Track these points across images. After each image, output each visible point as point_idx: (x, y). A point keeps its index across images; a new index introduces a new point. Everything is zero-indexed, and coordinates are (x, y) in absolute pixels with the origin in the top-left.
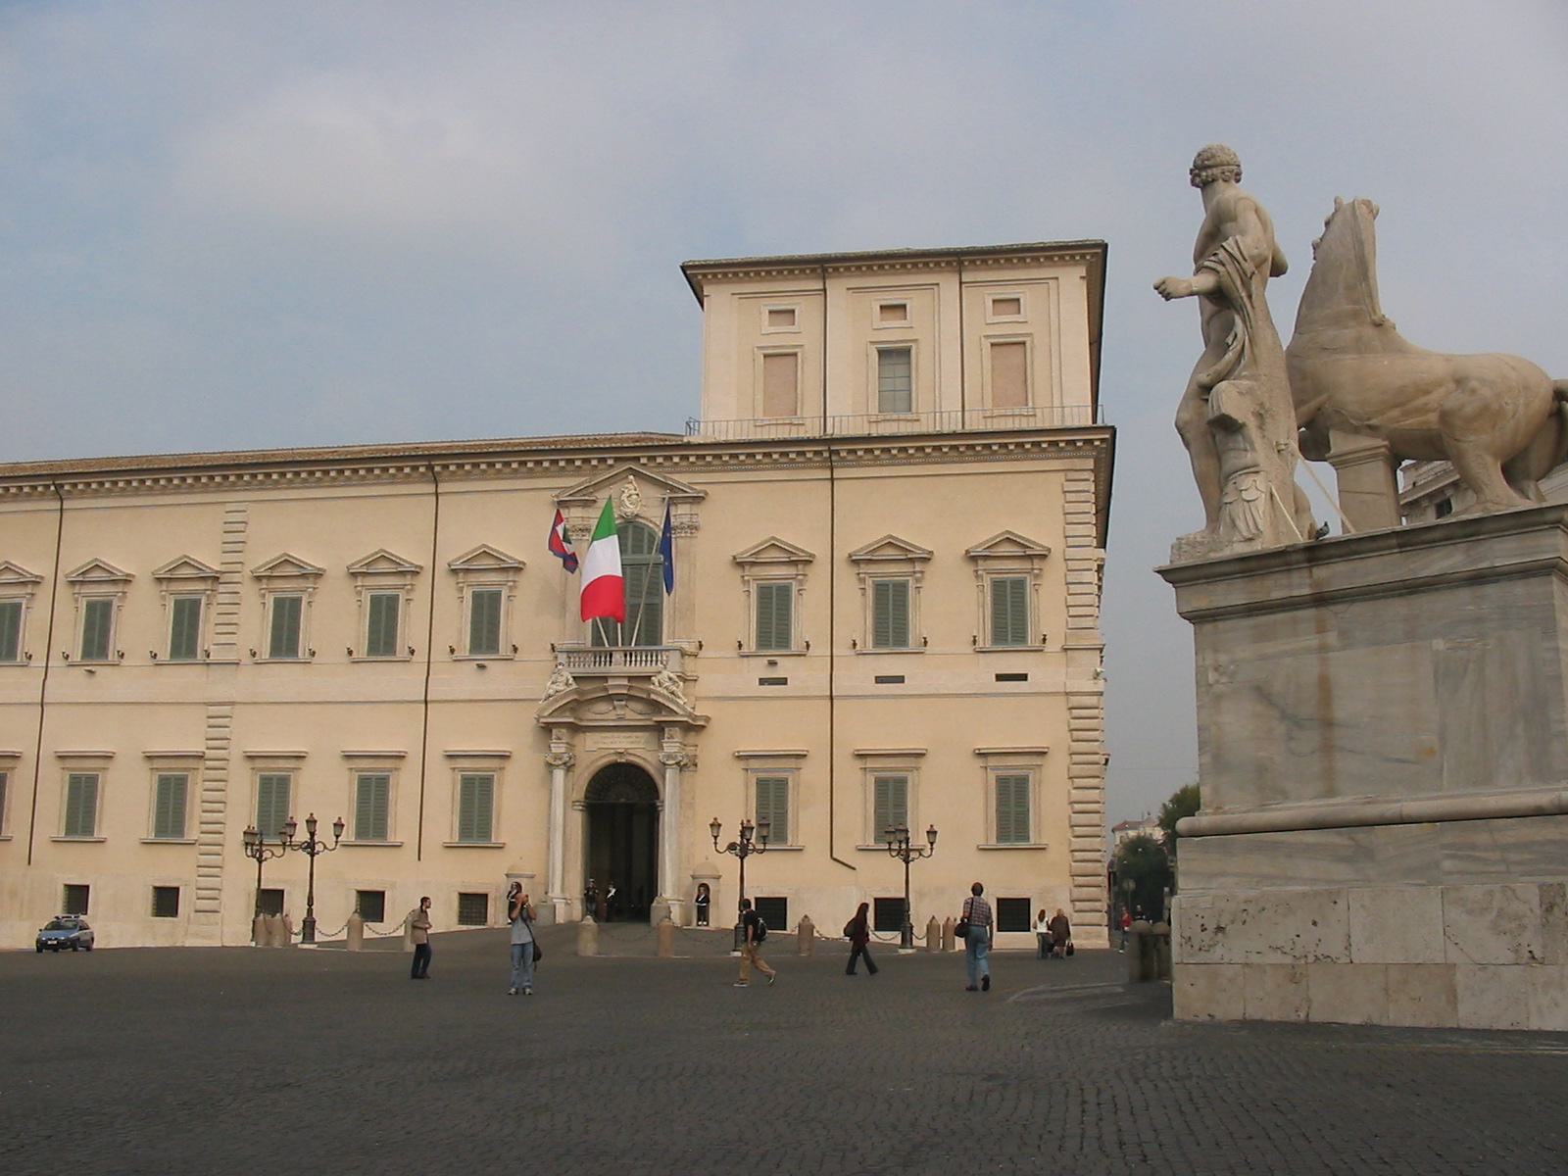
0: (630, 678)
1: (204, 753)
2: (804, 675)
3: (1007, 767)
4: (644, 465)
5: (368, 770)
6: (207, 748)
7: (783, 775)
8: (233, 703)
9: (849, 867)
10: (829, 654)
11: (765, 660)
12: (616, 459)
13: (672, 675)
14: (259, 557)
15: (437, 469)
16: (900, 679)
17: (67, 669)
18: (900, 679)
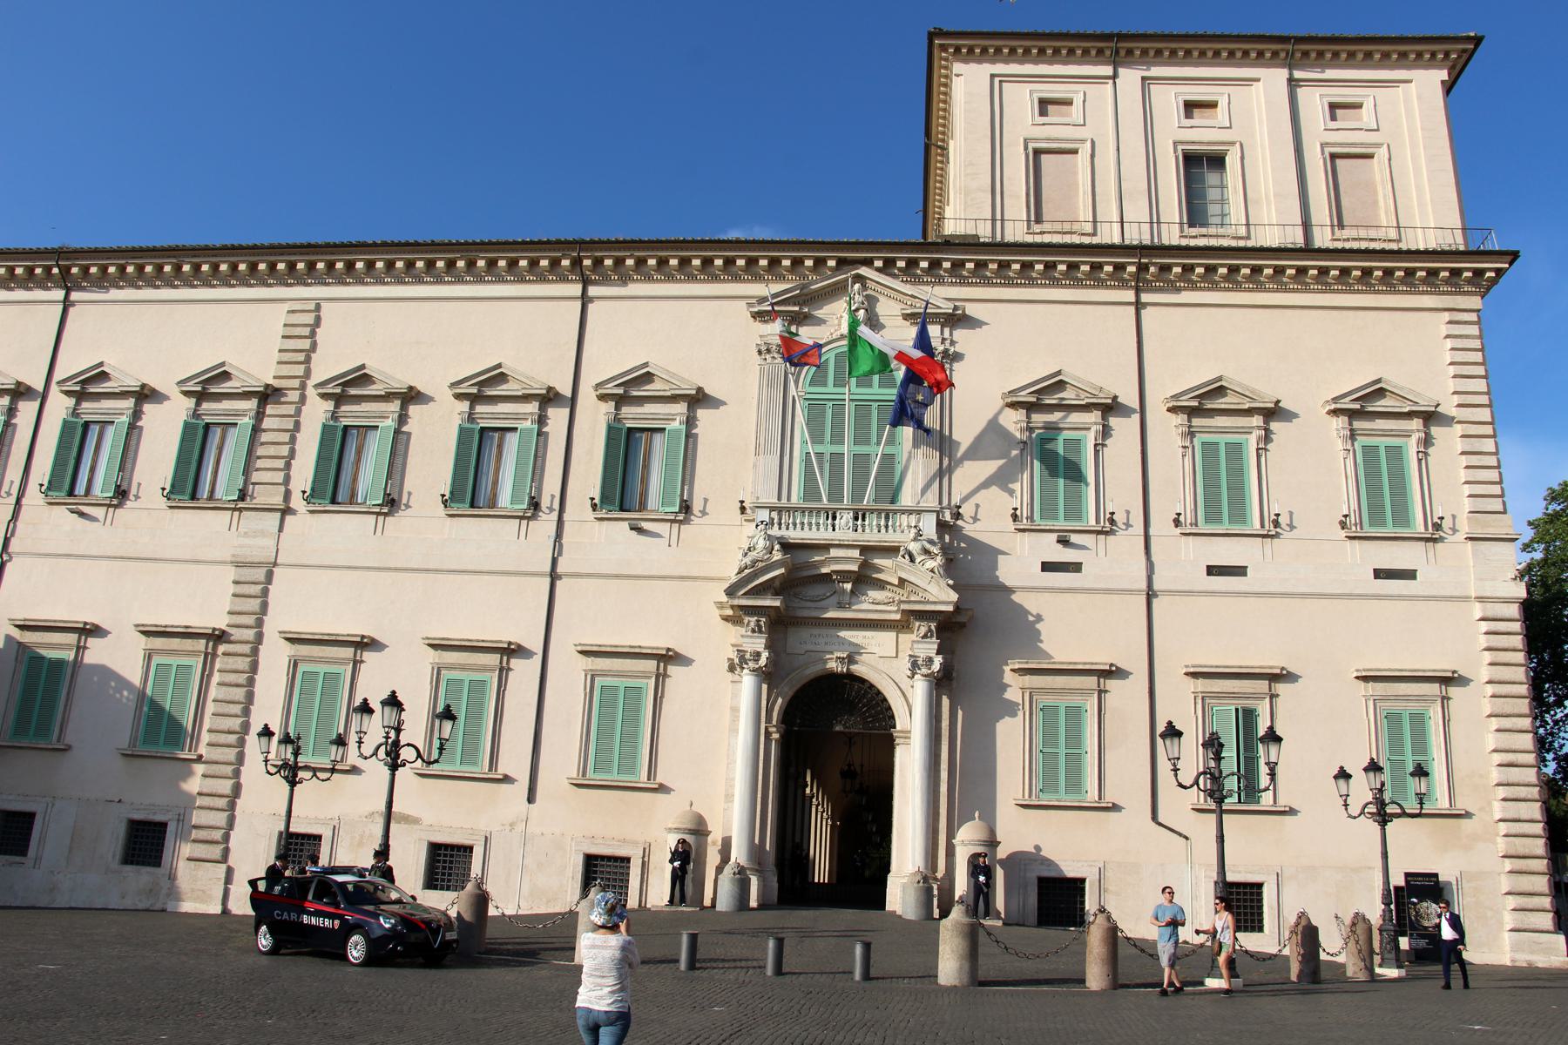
0: (865, 550)
1: (224, 632)
3: (1397, 698)
5: (463, 668)
7: (1075, 701)
9: (1180, 835)
11: (1054, 536)
12: (842, 262)
13: (928, 546)
14: (328, 365)
15: (587, 262)
16: (1240, 571)
18: (1240, 571)
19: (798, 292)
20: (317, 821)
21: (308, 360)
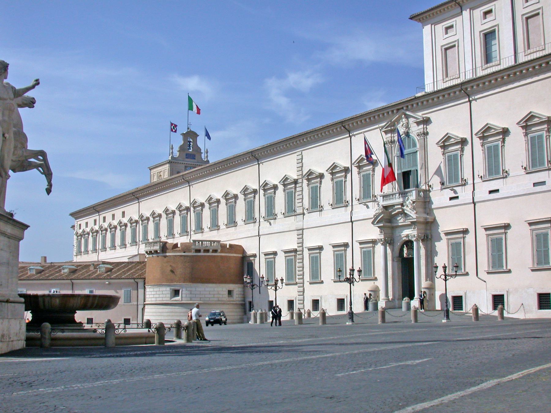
1: (296, 249)
2: (465, 194)
4: (405, 110)
6: (298, 247)
8: (303, 229)
10: (472, 183)
12: (398, 110)
15: (347, 127)
16: (497, 191)
17: (284, 218)
18: (497, 191)
19: (390, 123)
20: (318, 296)
21: (302, 170)
